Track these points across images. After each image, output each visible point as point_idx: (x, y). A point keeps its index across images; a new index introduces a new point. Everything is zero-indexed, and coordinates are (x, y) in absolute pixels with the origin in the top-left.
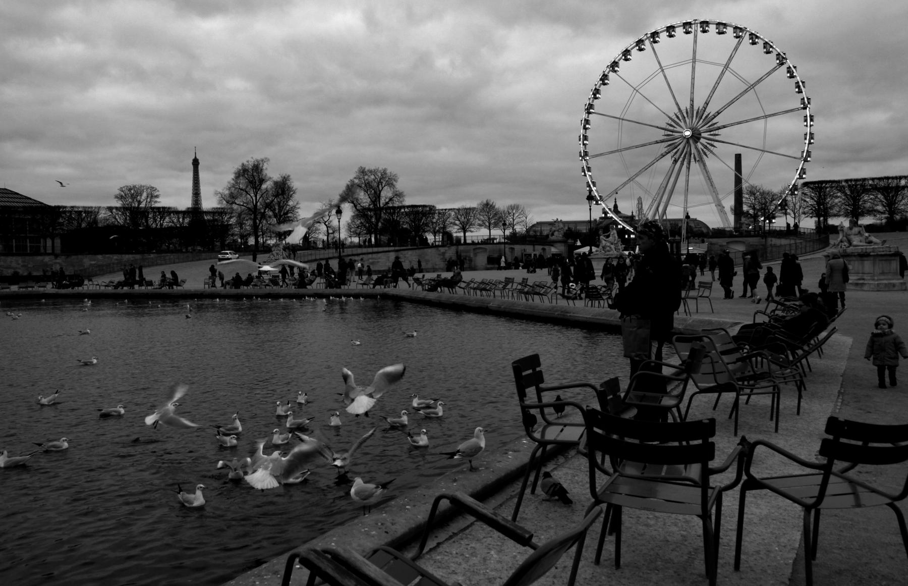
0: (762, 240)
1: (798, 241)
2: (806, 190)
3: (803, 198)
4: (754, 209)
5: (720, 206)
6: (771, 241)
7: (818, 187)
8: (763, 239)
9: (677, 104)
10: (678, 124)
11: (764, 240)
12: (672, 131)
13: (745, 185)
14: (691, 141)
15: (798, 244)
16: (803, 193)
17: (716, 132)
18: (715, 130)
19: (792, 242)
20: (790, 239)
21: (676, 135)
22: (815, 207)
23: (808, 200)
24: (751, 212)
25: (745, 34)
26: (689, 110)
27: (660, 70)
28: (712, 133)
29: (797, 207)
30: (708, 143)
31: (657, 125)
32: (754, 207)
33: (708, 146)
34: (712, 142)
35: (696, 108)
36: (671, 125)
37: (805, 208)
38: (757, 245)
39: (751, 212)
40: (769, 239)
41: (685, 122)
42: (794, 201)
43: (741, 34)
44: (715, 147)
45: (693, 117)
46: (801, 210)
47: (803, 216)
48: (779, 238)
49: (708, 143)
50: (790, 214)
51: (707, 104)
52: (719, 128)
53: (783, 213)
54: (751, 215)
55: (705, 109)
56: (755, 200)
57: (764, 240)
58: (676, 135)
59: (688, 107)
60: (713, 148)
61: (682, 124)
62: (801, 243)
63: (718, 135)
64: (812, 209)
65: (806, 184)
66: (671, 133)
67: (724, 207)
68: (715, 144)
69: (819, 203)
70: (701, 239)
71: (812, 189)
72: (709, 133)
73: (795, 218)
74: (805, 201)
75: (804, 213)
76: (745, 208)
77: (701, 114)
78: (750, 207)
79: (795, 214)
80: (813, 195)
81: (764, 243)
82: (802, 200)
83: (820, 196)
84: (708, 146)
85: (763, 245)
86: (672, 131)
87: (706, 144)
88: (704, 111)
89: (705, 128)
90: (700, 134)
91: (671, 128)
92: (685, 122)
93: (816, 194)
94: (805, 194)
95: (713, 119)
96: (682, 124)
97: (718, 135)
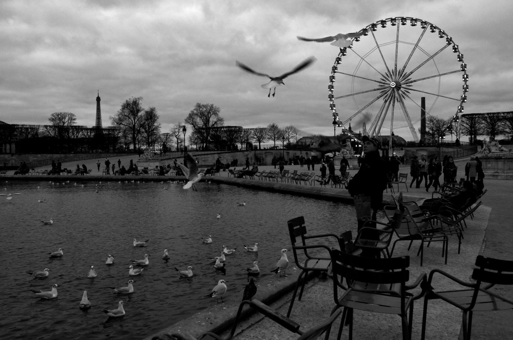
0: (437, 149)
1: (459, 150)
2: (464, 119)
3: (462, 124)
4: (433, 130)
6: (443, 149)
7: (471, 117)
8: (438, 148)
11: (438, 149)
13: (427, 116)
15: (458, 151)
16: (462, 121)
17: (410, 84)
18: (409, 83)
19: (455, 150)
20: (454, 148)
22: (469, 129)
23: (465, 125)
24: (431, 132)
26: (394, 71)
28: (408, 85)
29: (458, 129)
30: (405, 91)
32: (432, 129)
33: (405, 92)
34: (408, 90)
35: (398, 70)
37: (463, 130)
38: (434, 152)
39: (431, 132)
40: (441, 148)
42: (456, 126)
44: (409, 93)
45: (396, 75)
46: (460, 131)
47: (462, 134)
48: (447, 147)
49: (405, 91)
51: (405, 68)
52: (412, 82)
54: (430, 133)
55: (404, 70)
56: (433, 125)
57: (438, 149)
59: (394, 69)
60: (408, 93)
62: (461, 151)
63: (411, 86)
64: (467, 131)
65: (464, 116)
69: (471, 127)
70: (400, 148)
71: (467, 118)
72: (406, 85)
73: (457, 136)
74: (463, 126)
75: (462, 133)
76: (427, 130)
77: (401, 73)
78: (430, 129)
79: (457, 133)
80: (468, 122)
81: (438, 151)
82: (461, 125)
83: (472, 123)
84: (405, 92)
85: (438, 152)
87: (404, 91)
88: (403, 71)
89: (403, 82)
93: (470, 122)
94: (463, 122)
95: (408, 76)
97: (411, 86)
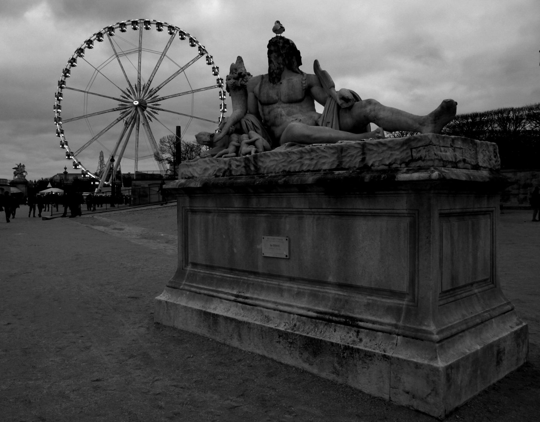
10: (134, 93)
12: (128, 96)
14: (139, 109)
17: (157, 111)
21: (130, 100)
28: (153, 110)
34: (151, 117)
35: (150, 88)
36: (129, 91)
52: (159, 109)
60: (150, 121)
66: (126, 97)
68: (152, 119)
72: (151, 109)
86: (128, 96)
90: (145, 108)
91: (129, 94)
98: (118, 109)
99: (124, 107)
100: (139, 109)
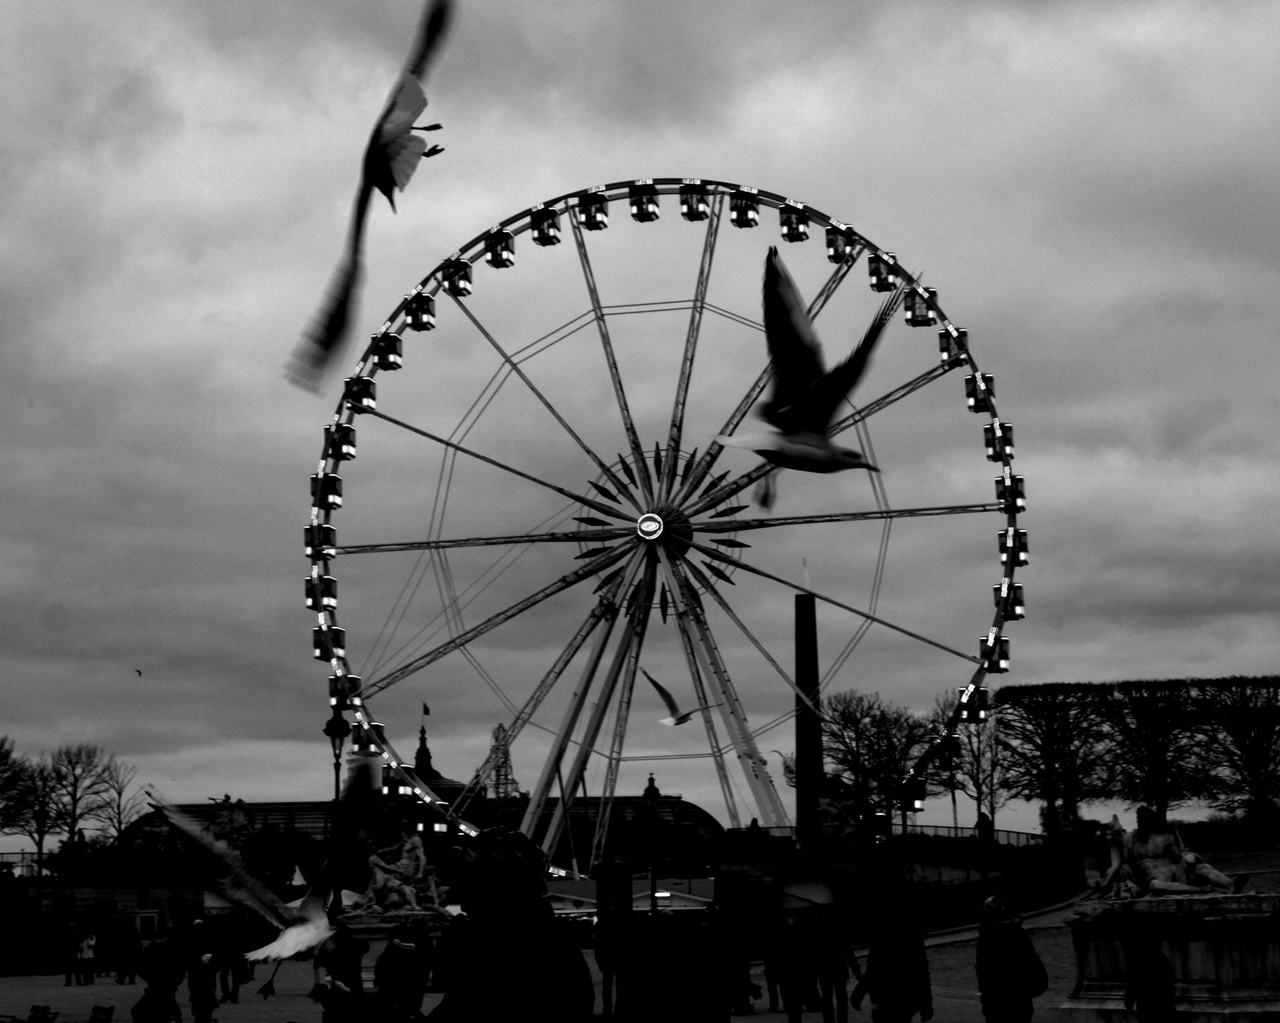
2: (1011, 714)
3: (1002, 736)
5: (753, 759)
9: (631, 429)
14: (661, 553)
21: (617, 524)
23: (1015, 743)
25: (859, 253)
27: (592, 316)
29: (986, 765)
31: (560, 486)
37: (1008, 769)
39: (847, 778)
41: (648, 486)
42: (975, 745)
43: (848, 249)
46: (997, 775)
47: (1003, 793)
50: (963, 787)
53: (942, 783)
58: (617, 524)
61: (638, 494)
67: (764, 763)
73: (979, 800)
74: (1007, 747)
75: (1005, 784)
76: (830, 766)
77: (700, 471)
79: (978, 786)
82: (998, 742)
89: (704, 518)
92: (648, 486)
96: (638, 494)
98: (579, 577)
99: (601, 558)
100: (661, 553)
